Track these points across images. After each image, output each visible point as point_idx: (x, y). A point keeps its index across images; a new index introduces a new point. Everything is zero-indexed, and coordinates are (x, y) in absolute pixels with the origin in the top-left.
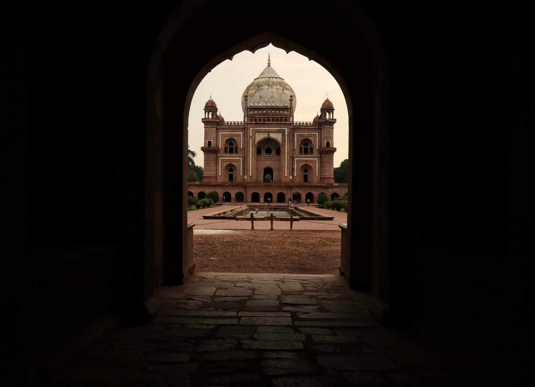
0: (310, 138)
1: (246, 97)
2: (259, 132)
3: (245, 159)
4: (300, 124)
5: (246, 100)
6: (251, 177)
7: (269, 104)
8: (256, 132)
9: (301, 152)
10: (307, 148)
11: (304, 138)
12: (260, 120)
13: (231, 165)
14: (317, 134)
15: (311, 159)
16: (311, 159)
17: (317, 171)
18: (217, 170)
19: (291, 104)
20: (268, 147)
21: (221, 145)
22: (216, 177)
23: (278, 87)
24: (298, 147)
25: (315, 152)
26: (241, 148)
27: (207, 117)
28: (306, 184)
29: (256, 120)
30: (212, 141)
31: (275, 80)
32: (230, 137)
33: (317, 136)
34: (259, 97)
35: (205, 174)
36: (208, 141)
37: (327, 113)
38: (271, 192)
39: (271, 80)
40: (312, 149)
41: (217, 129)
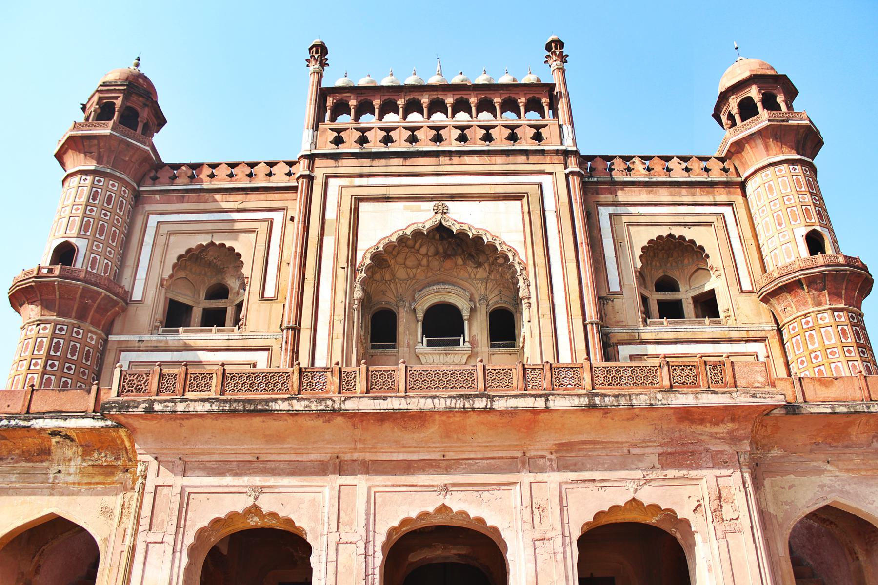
0: (689, 234)
14: (727, 211)
30: (81, 245)
32: (204, 240)
41: (138, 198)
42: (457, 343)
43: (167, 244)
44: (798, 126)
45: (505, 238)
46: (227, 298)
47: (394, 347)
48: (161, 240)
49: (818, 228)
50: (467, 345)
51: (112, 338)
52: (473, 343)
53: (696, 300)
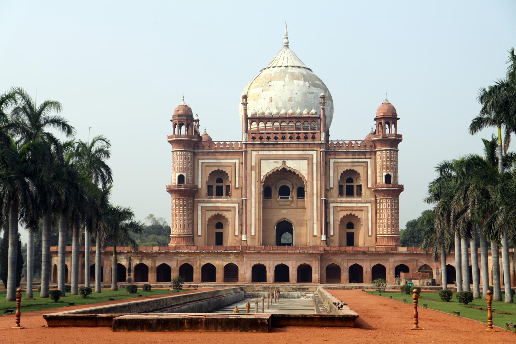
0: (355, 169)
3: (244, 204)
4: (338, 143)
5: (245, 104)
6: (253, 237)
7: (282, 112)
8: (261, 159)
9: (341, 193)
10: (353, 186)
12: (268, 138)
14: (369, 161)
16: (360, 205)
21: (201, 182)
22: (193, 239)
23: (301, 82)
24: (336, 184)
27: (176, 133)
28: (350, 249)
29: (261, 138)
30: (185, 175)
31: (295, 70)
32: (217, 169)
34: (267, 100)
35: (174, 232)
36: (178, 174)
37: (387, 126)
39: (290, 70)
40: (360, 187)
41: (194, 153)
42: (288, 198)
43: (206, 170)
44: (391, 139)
45: (302, 172)
46: (222, 182)
47: (271, 198)
48: (204, 169)
49: (390, 173)
50: (291, 199)
51: (195, 199)
52: (292, 198)
53: (358, 186)
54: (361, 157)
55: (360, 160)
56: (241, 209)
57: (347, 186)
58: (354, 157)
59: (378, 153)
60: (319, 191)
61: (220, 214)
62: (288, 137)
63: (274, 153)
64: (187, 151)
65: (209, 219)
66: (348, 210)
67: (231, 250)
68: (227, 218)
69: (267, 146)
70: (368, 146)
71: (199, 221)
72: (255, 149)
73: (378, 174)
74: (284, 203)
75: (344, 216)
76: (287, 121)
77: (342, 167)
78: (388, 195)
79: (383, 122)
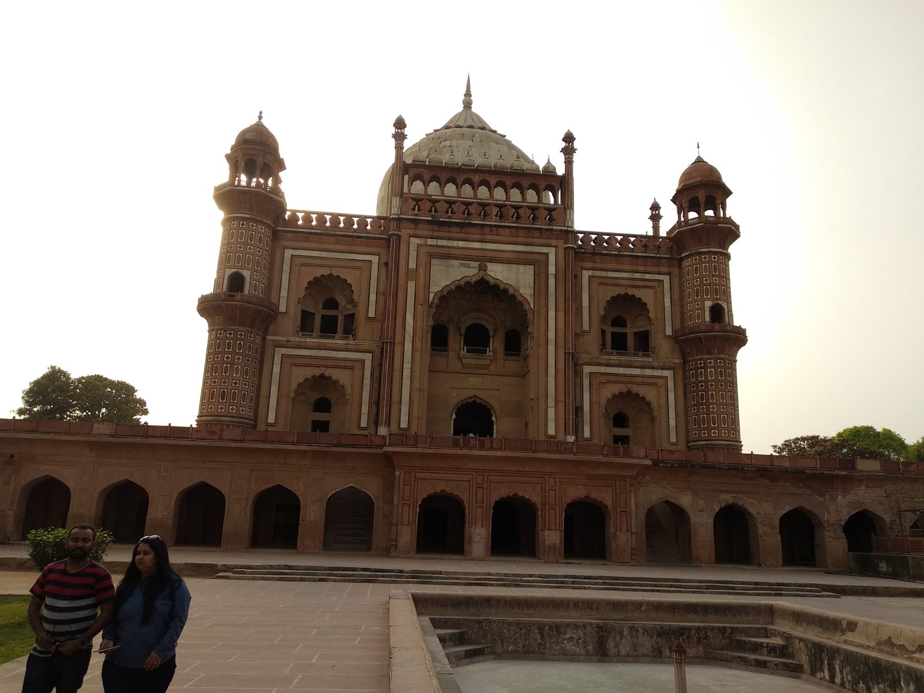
1: (400, 124)
2: (447, 256)
5: (399, 137)
8: (432, 256)
11: (617, 291)
13: (322, 381)
14: (666, 279)
15: (648, 372)
16: (648, 372)
17: (672, 422)
18: (258, 396)
19: (569, 163)
20: (480, 321)
21: (287, 298)
25: (663, 347)
26: (372, 314)
30: (246, 274)
32: (326, 272)
33: (667, 285)
36: (229, 272)
38: (532, 494)
43: (299, 273)
45: (521, 292)
47: (446, 351)
49: (720, 302)
50: (491, 354)
51: (268, 337)
53: (635, 333)
54: (649, 269)
55: (648, 276)
56: (378, 368)
57: (612, 333)
58: (635, 268)
59: (686, 263)
60: (561, 334)
61: (327, 375)
62: (494, 213)
63: (461, 244)
64: (257, 221)
65: (300, 385)
66: (624, 383)
67: (354, 446)
68: (343, 386)
69: (447, 228)
70: (663, 249)
71: (274, 389)
72: (419, 232)
73: (688, 307)
74: (476, 361)
75: (614, 396)
76: (493, 180)
77: (609, 287)
78: (722, 351)
79: (701, 195)
